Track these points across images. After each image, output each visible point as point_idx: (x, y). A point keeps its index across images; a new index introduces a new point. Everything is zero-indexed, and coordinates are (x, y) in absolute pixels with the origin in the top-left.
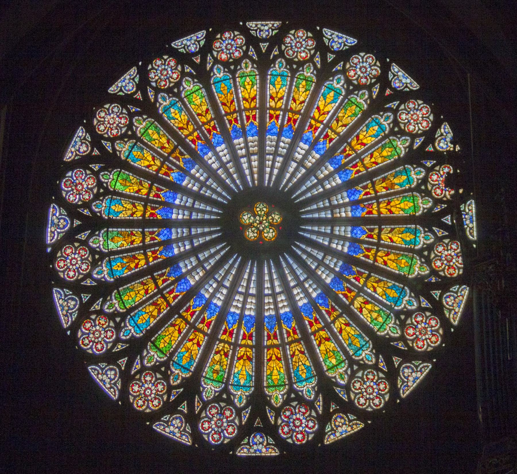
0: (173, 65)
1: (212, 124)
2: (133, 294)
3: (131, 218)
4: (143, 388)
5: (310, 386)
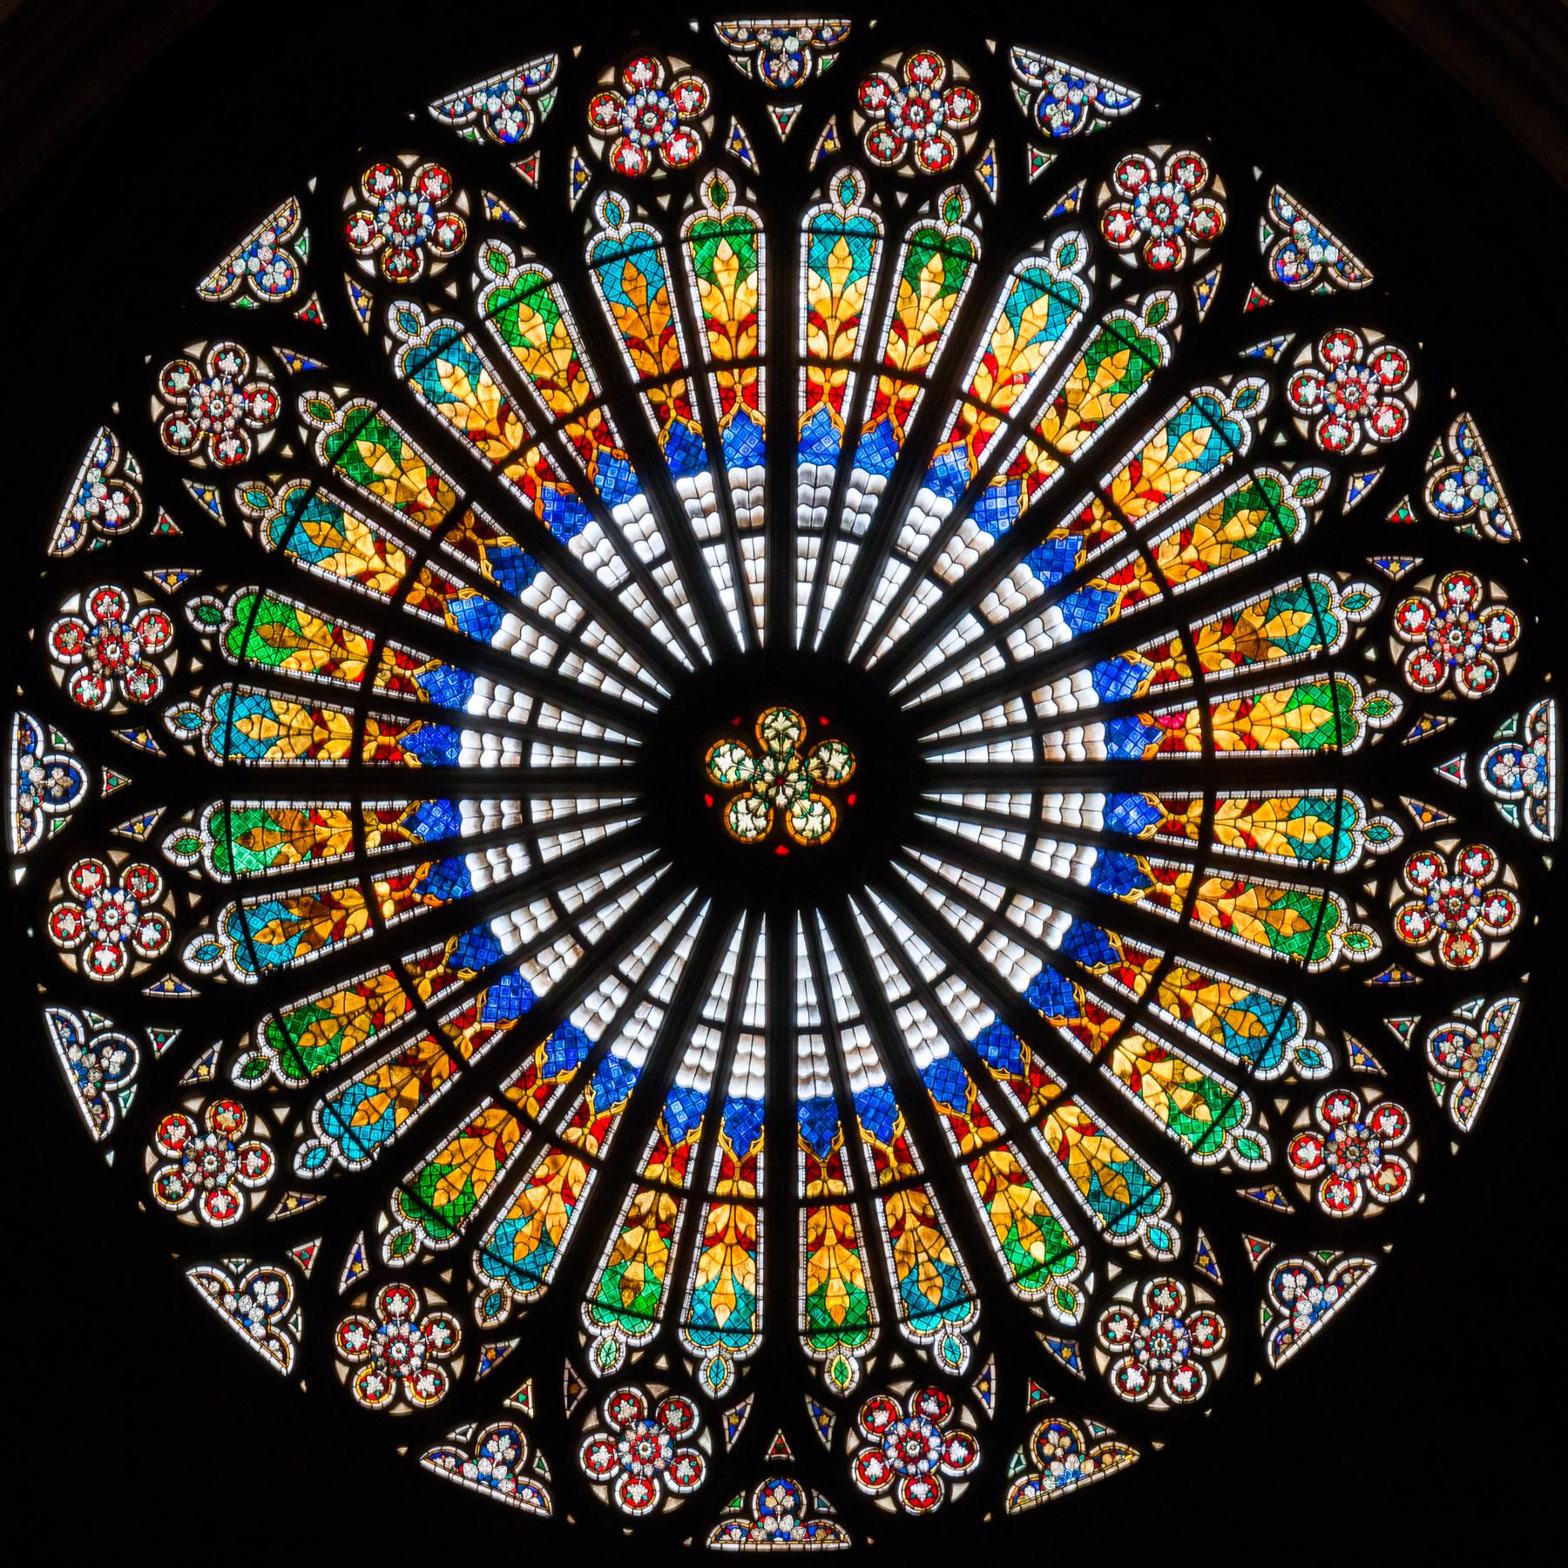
0: (438, 192)
1: (594, 419)
2: (331, 1027)
3: (310, 763)
4: (381, 1338)
5: (957, 1331)
